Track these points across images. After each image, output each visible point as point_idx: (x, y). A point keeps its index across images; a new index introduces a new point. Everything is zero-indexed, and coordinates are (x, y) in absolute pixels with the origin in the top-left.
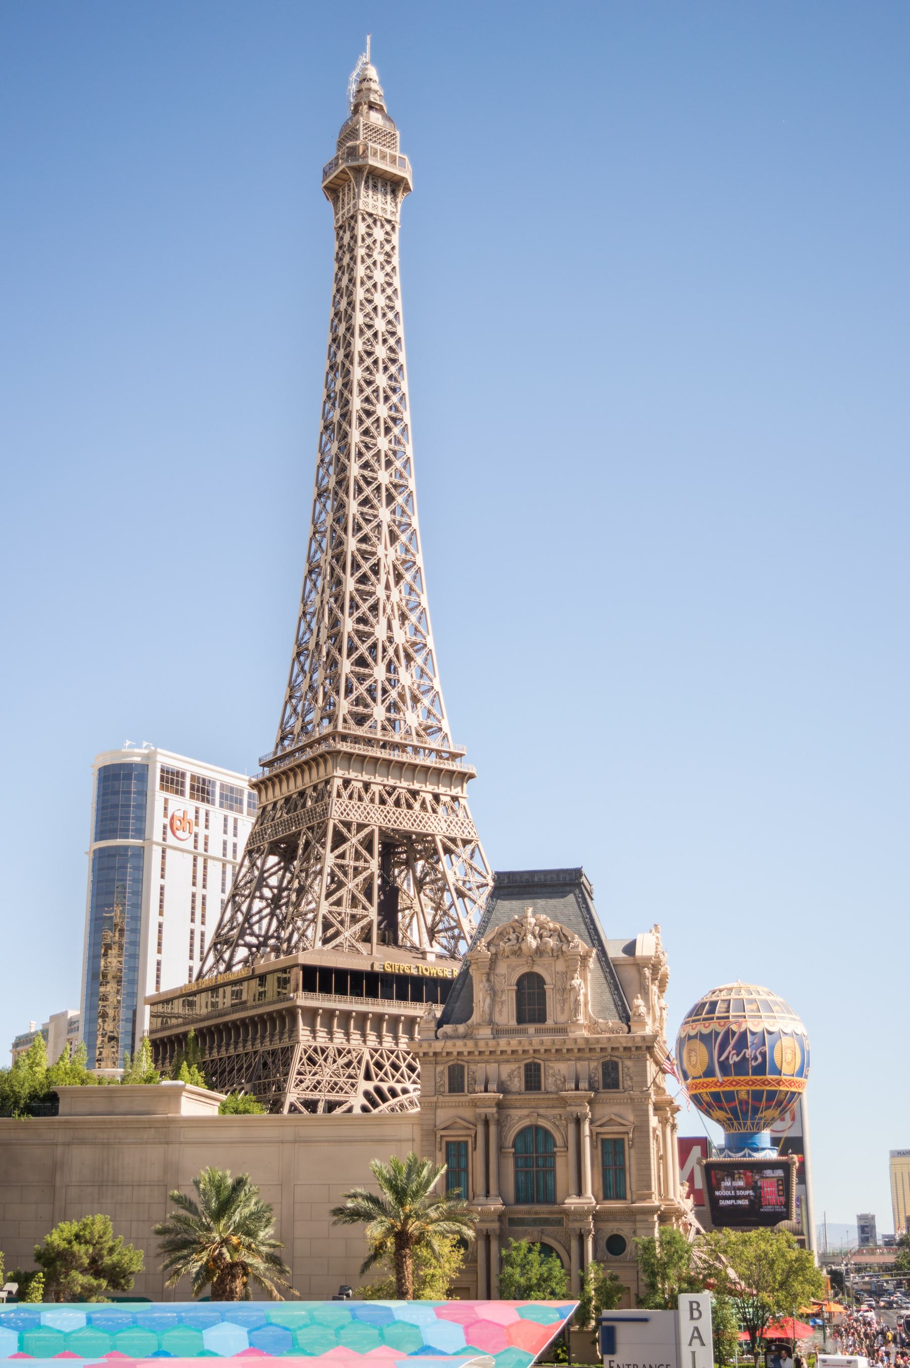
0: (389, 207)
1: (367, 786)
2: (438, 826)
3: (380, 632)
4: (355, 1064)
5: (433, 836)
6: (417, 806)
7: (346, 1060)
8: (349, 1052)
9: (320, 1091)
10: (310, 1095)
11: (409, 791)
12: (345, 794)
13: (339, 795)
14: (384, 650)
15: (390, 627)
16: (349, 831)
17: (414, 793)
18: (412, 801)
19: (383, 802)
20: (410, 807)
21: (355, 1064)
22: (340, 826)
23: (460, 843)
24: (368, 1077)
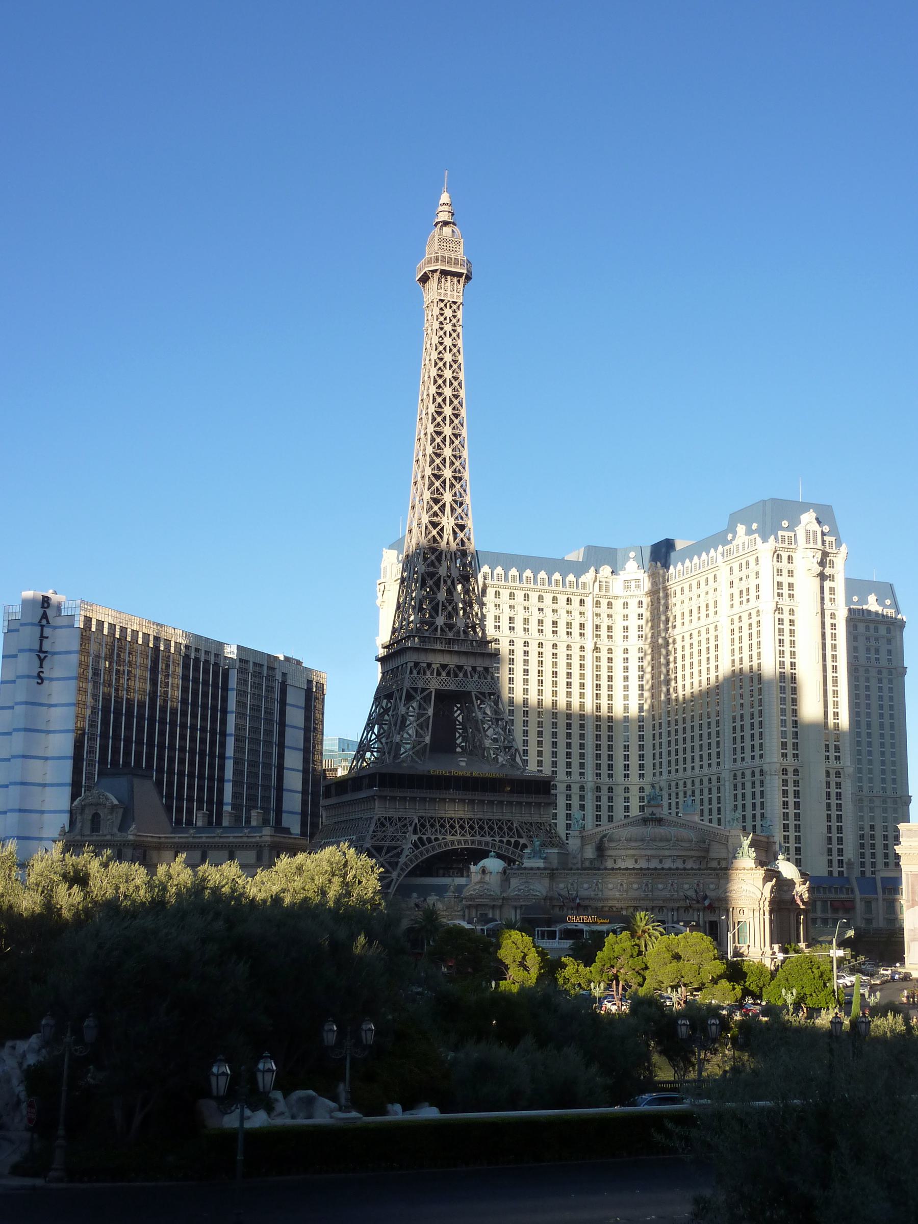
0: (455, 293)
1: (429, 665)
2: (472, 686)
3: (442, 571)
6: (461, 675)
11: (457, 666)
13: (411, 672)
14: (445, 581)
16: (416, 692)
17: (460, 668)
18: (458, 672)
19: (439, 674)
20: (456, 676)
23: (487, 695)
24: (415, 832)
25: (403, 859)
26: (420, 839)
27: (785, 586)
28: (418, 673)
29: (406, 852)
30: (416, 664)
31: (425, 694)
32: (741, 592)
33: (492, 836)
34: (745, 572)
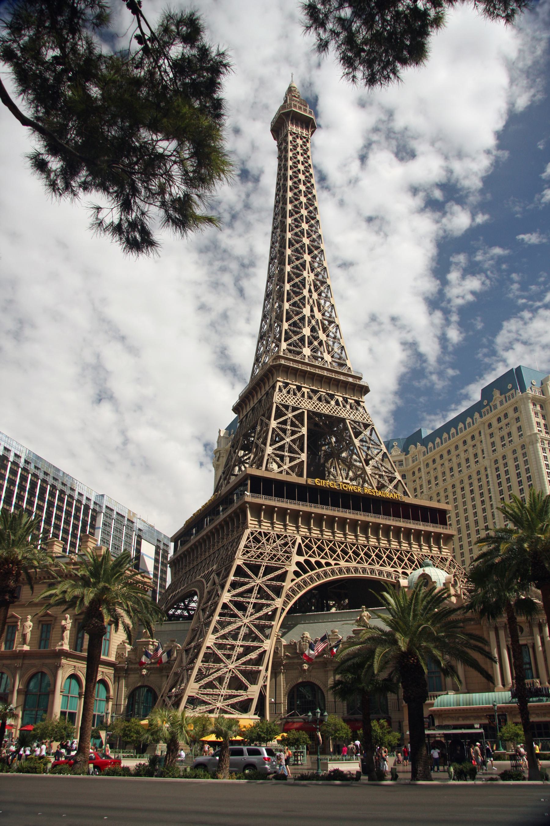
3: (306, 311)
4: (290, 544)
5: (343, 420)
6: (333, 403)
7: (283, 542)
8: (286, 537)
9: (262, 559)
10: (253, 561)
11: (327, 394)
12: (284, 391)
14: (310, 322)
15: (312, 311)
18: (329, 400)
20: (328, 402)
21: (290, 544)
22: (280, 406)
25: (287, 585)
26: (307, 561)
27: (542, 426)
28: (288, 392)
29: (290, 576)
30: (286, 384)
31: (296, 413)
32: (502, 438)
33: (392, 567)
34: (504, 422)
